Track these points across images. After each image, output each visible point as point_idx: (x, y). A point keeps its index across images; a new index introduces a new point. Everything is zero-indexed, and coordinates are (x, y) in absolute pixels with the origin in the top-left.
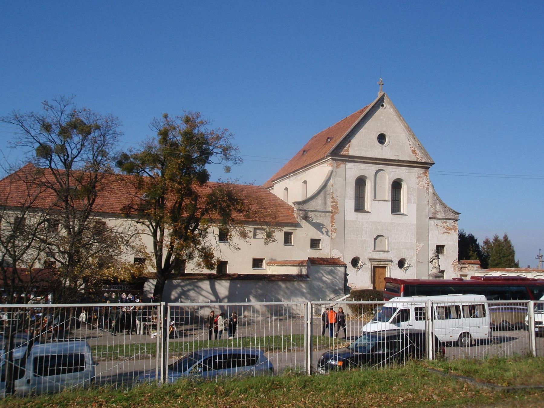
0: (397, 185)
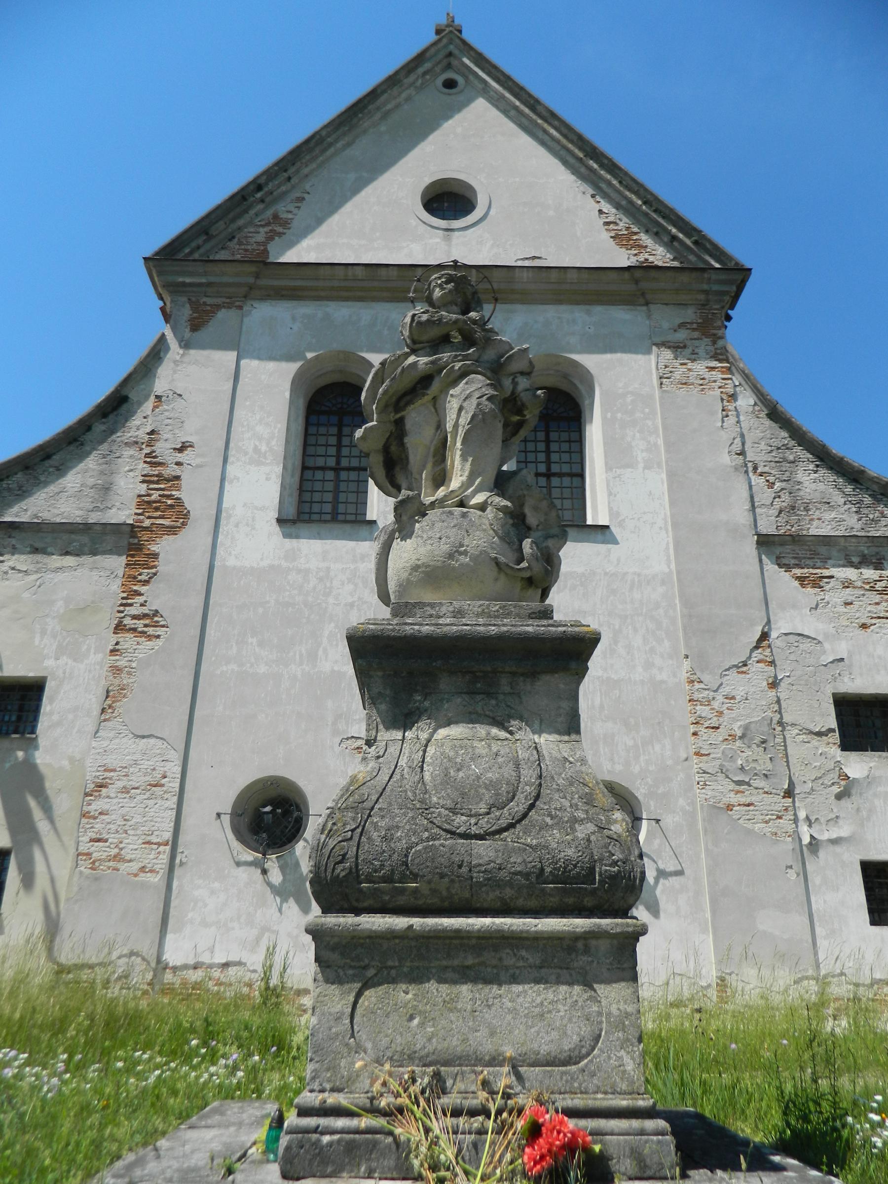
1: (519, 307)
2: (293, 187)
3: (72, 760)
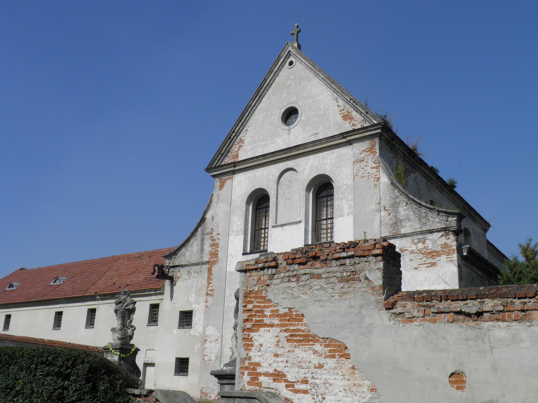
2: (245, 126)
3: (199, 333)
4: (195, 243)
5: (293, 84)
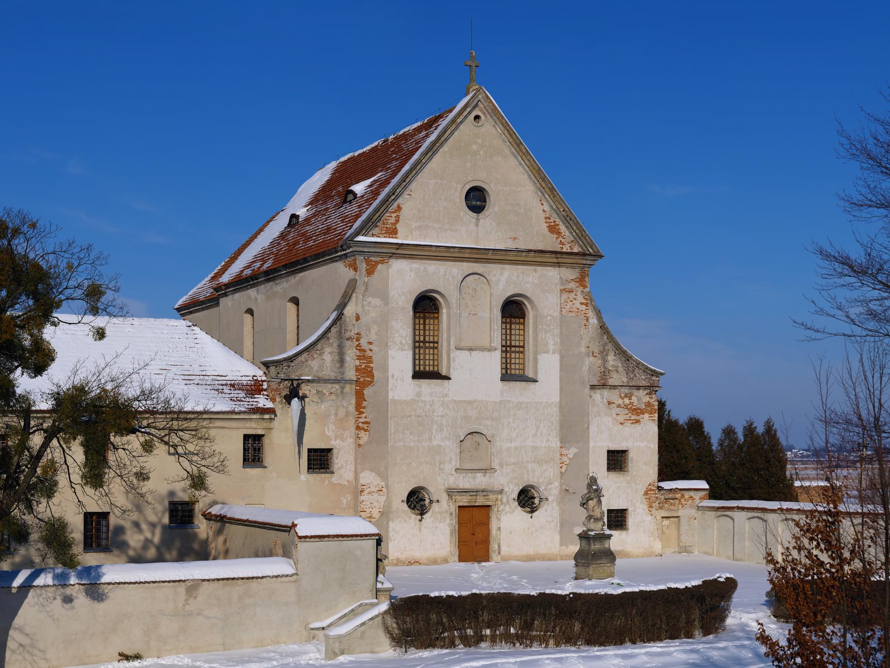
0: (513, 310)
1: (507, 266)
3: (348, 481)
4: (328, 350)
5: (482, 153)
